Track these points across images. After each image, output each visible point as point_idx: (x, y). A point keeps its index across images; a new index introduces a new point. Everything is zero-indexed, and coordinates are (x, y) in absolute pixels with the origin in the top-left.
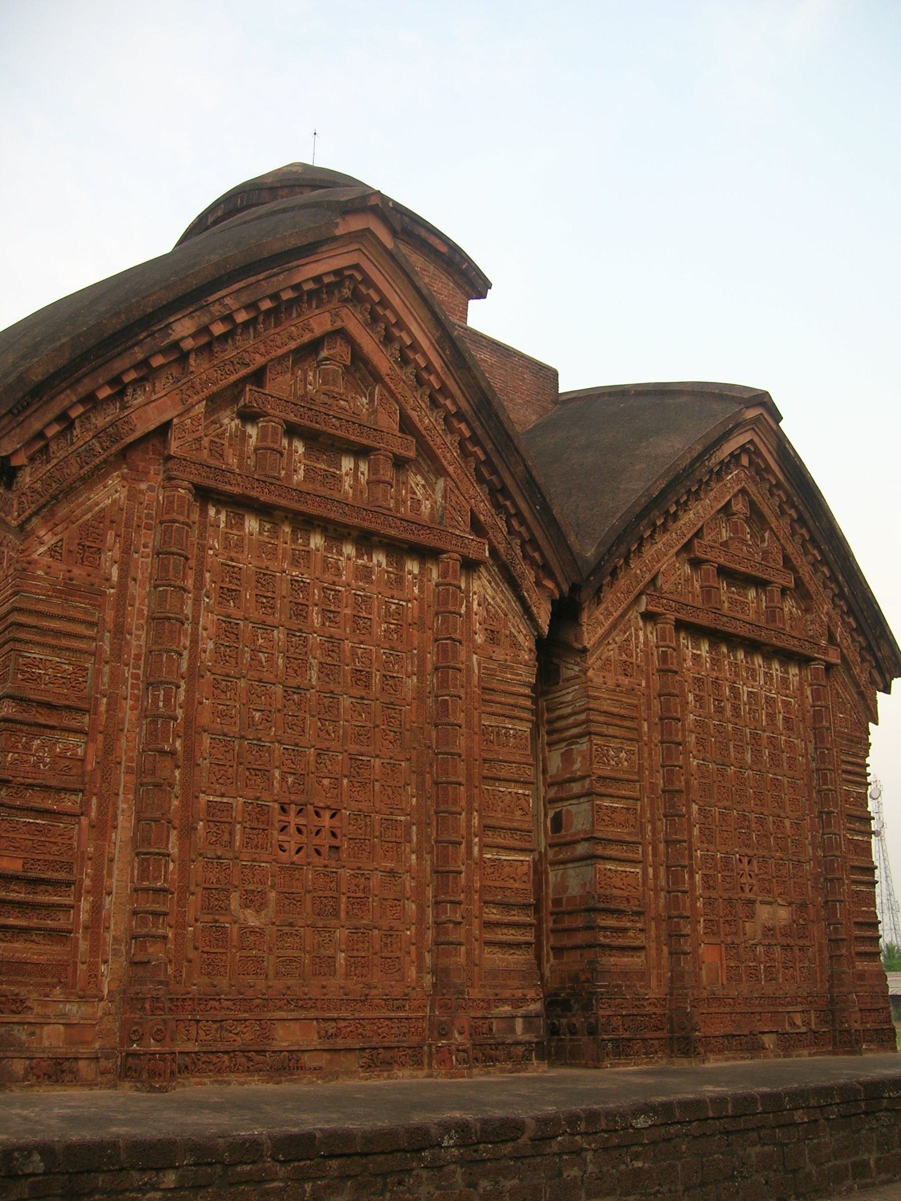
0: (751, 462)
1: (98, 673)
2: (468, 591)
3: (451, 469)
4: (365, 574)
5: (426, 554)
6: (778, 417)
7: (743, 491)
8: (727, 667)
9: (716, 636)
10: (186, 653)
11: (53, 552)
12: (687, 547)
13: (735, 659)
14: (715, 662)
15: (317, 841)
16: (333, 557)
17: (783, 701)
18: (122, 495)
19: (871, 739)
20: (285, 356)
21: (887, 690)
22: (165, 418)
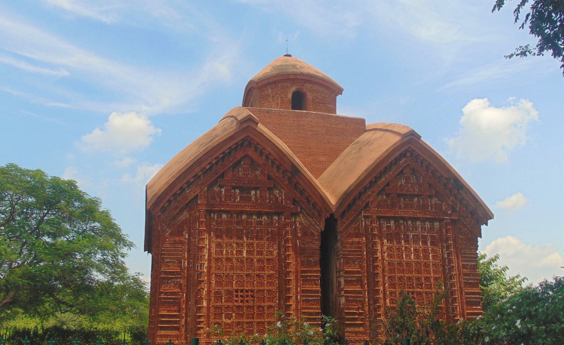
0: (411, 154)
1: (184, 262)
2: (295, 221)
3: (285, 188)
4: (260, 223)
5: (279, 214)
6: (419, 137)
7: (408, 165)
8: (402, 228)
9: (396, 219)
10: (207, 254)
11: (170, 234)
12: (383, 190)
13: (407, 223)
14: (397, 226)
15: (246, 299)
16: (249, 220)
17: (430, 236)
18: (187, 216)
19: (479, 244)
20: (231, 166)
21: (487, 224)
22: (196, 194)
